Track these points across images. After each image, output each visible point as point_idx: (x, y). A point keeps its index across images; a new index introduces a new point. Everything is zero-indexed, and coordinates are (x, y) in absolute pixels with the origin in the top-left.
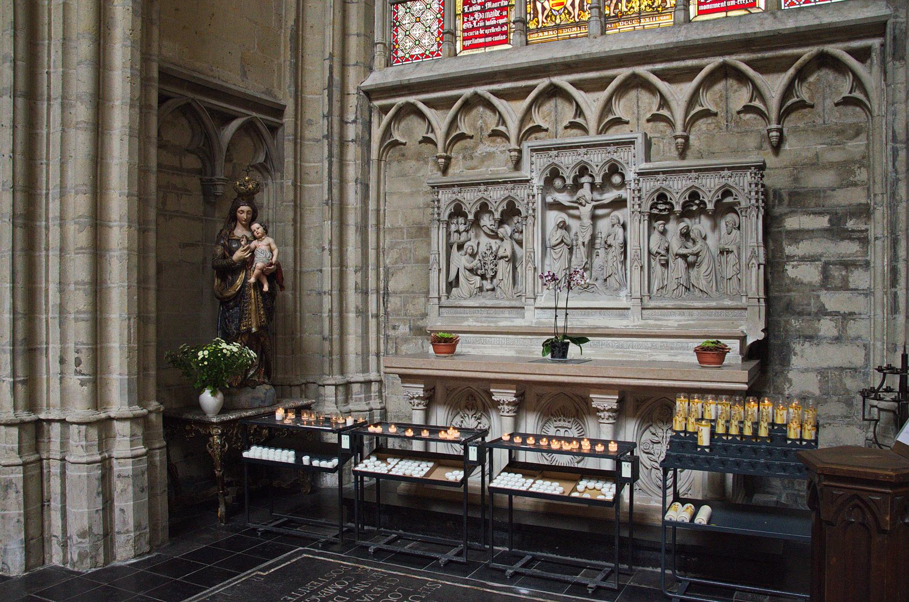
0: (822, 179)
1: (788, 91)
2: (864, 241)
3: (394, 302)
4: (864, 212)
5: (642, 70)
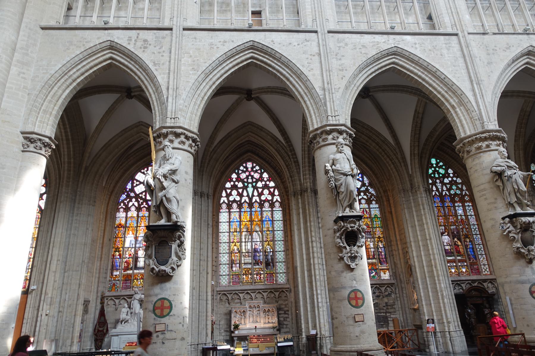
0: (283, 306)
1: (279, 295)
2: (288, 314)
3: (221, 326)
4: (288, 311)
5: (260, 291)
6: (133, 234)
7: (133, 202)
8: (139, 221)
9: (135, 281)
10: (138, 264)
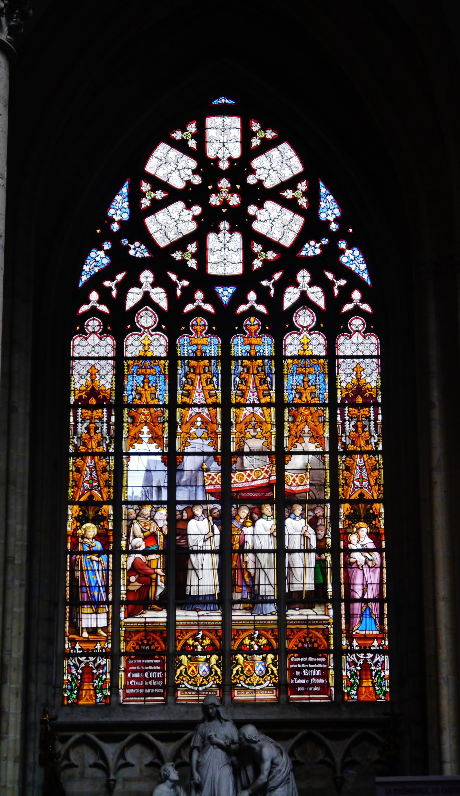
6: (155, 438)
7: (147, 287)
8: (181, 379)
9: (184, 658)
10: (192, 579)
